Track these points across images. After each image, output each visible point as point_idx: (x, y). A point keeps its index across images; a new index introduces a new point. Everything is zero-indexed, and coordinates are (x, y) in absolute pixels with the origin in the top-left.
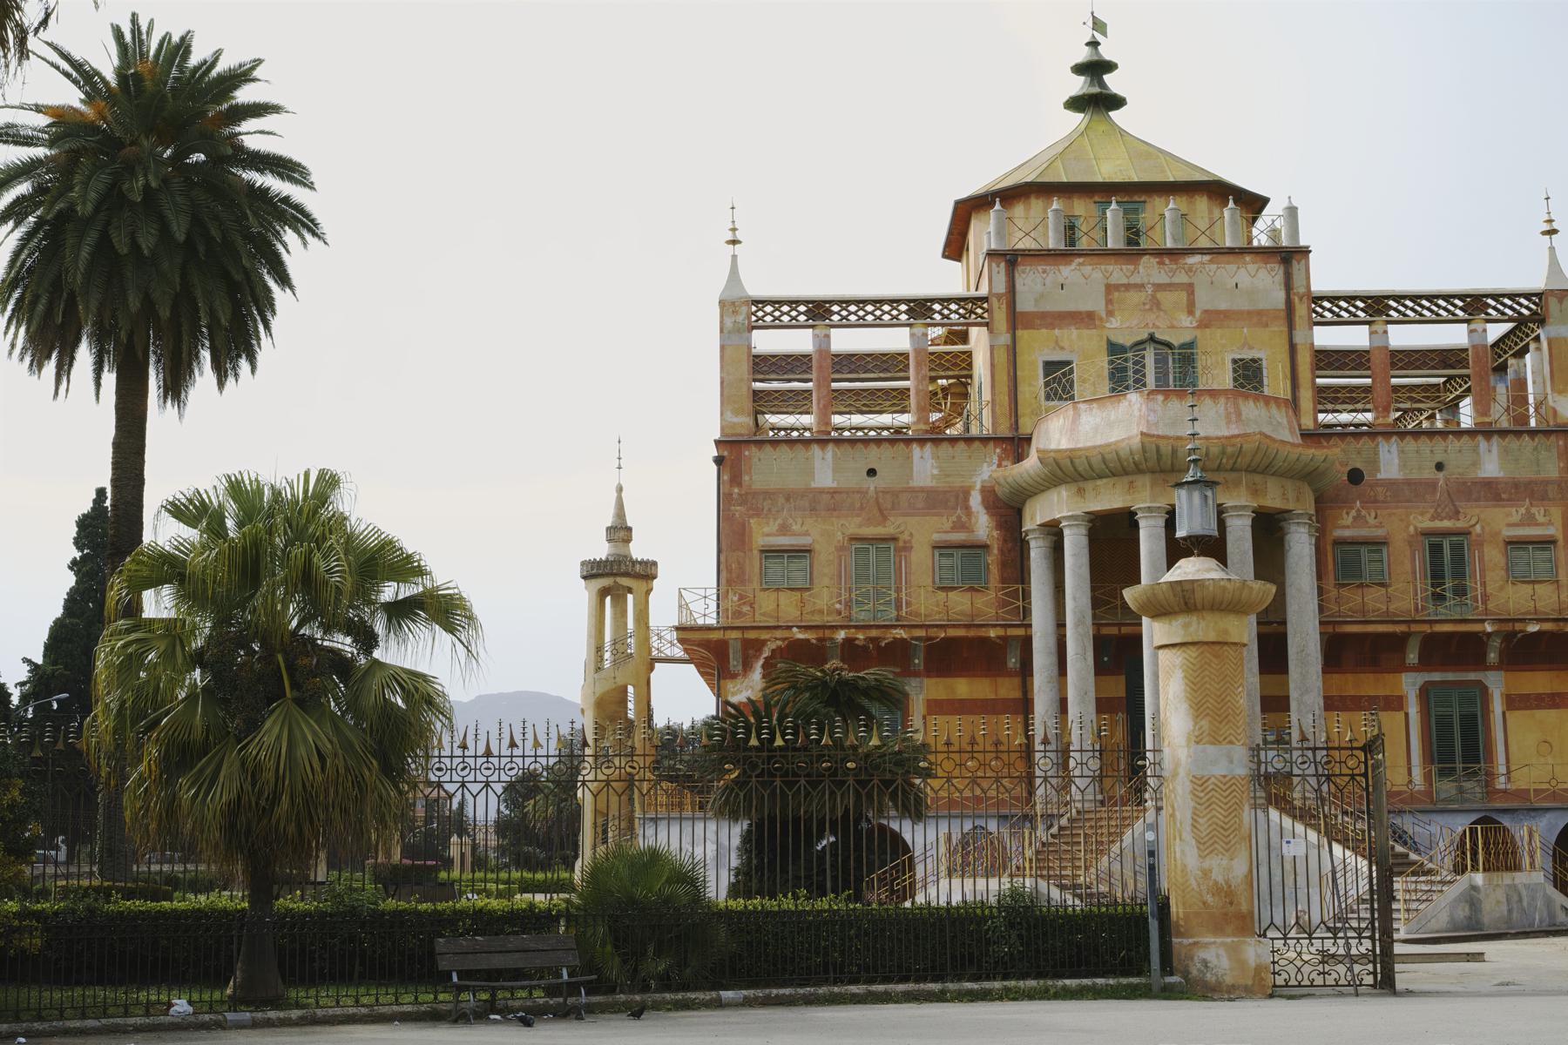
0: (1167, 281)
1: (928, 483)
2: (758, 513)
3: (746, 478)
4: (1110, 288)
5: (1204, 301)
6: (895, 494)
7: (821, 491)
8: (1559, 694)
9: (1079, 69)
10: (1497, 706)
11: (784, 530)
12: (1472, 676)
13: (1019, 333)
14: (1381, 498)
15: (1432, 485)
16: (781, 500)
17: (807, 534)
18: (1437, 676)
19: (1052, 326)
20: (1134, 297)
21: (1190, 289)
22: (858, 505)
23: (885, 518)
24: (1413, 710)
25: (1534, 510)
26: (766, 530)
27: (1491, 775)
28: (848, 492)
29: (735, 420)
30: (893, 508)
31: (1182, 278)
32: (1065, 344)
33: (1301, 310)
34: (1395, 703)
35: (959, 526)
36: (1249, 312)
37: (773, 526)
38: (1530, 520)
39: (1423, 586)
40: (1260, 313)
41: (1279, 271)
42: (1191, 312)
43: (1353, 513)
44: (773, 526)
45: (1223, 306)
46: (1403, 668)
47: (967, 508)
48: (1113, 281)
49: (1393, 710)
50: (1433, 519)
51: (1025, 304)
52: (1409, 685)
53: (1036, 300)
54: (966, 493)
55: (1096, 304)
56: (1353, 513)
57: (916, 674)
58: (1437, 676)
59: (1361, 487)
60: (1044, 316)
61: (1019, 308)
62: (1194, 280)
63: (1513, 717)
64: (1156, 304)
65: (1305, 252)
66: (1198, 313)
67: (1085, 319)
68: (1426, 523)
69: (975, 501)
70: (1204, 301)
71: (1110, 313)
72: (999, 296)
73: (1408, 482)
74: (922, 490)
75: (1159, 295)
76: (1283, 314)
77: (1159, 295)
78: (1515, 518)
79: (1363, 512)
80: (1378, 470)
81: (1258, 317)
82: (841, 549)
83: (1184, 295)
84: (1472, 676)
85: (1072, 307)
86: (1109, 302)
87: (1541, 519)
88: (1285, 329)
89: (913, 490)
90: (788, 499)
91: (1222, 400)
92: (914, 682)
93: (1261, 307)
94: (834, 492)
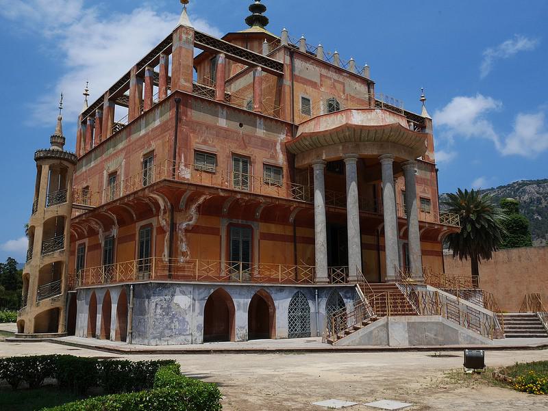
2: (194, 131)
9: (254, 8)
11: (205, 142)
16: (204, 128)
17: (214, 146)
19: (304, 84)
20: (329, 82)
23: (246, 147)
32: (308, 92)
33: (372, 103)
37: (199, 140)
44: (199, 140)
47: (276, 150)
55: (317, 80)
64: (335, 87)
67: (314, 85)
69: (278, 147)
71: (321, 85)
74: (260, 138)
75: (336, 84)
77: (336, 84)
82: (229, 157)
85: (309, 78)
86: (321, 81)
94: (226, 130)
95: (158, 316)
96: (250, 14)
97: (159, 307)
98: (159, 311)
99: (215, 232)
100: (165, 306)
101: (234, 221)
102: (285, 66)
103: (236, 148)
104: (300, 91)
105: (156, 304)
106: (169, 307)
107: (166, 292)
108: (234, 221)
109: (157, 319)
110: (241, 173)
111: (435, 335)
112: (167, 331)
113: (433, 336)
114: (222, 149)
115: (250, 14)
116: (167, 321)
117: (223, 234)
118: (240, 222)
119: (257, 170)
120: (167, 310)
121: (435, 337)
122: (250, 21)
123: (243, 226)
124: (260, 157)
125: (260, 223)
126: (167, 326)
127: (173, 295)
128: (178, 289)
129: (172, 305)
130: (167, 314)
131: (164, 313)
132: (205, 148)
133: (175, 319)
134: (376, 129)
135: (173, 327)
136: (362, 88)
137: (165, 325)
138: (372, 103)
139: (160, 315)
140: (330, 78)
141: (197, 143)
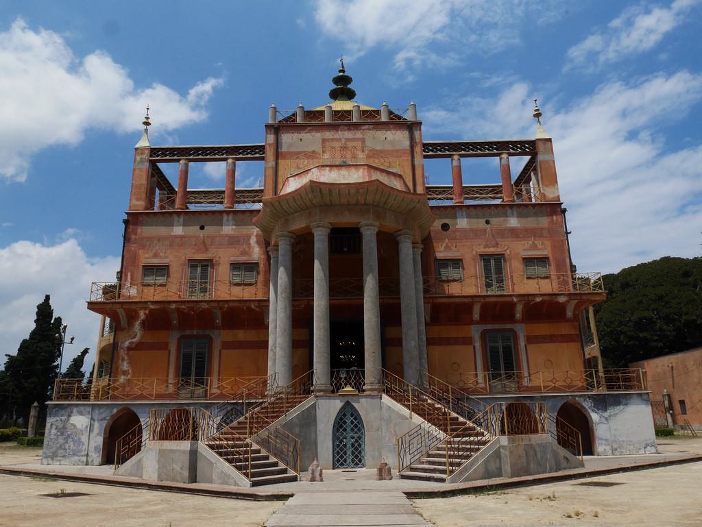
0: (352, 137)
2: (143, 247)
4: (324, 141)
7: (176, 237)
8: (554, 335)
9: (337, 80)
10: (522, 343)
11: (156, 256)
12: (508, 326)
13: (280, 161)
14: (458, 237)
15: (485, 231)
16: (156, 241)
17: (167, 257)
18: (489, 327)
21: (363, 141)
22: (194, 243)
23: (207, 250)
24: (478, 345)
25: (536, 242)
26: (147, 256)
27: (520, 377)
29: (137, 203)
30: (211, 245)
32: (301, 166)
33: (418, 149)
34: (468, 341)
35: (244, 253)
36: (392, 151)
38: (534, 247)
39: (482, 282)
40: (397, 151)
41: (406, 133)
43: (444, 245)
45: (379, 148)
46: (471, 322)
48: (325, 137)
49: (467, 344)
50: (485, 247)
51: (284, 149)
52: (475, 331)
53: (288, 147)
55: (317, 147)
56: (444, 245)
57: (218, 328)
58: (489, 327)
59: (448, 232)
63: (531, 347)
65: (420, 124)
66: (366, 152)
68: (482, 250)
70: (370, 144)
71: (324, 152)
72: (270, 145)
73: (472, 230)
74: (227, 235)
76: (409, 151)
78: (527, 246)
79: (450, 244)
80: (457, 224)
81: (397, 153)
83: (359, 144)
84: (508, 326)
87: (540, 247)
88: (410, 158)
90: (159, 241)
91: (361, 170)
92: (216, 332)
95: (52, 437)
96: (334, 86)
97: (54, 427)
98: (54, 431)
99: (164, 347)
100: (61, 426)
101: (188, 332)
102: (268, 148)
103: (194, 253)
105: (52, 425)
106: (64, 428)
107: (63, 412)
108: (188, 332)
109: (51, 439)
110: (198, 280)
111: (181, 468)
112: (61, 452)
113: (179, 469)
114: (175, 259)
115: (334, 86)
116: (61, 441)
117: (173, 348)
118: (195, 333)
119: (222, 272)
120: (62, 430)
121: (181, 472)
124: (225, 257)
125: (222, 331)
126: (61, 447)
127: (69, 416)
128: (75, 410)
129: (68, 426)
130: (62, 434)
131: (59, 434)
132: (155, 262)
133: (70, 440)
134: (358, 185)
135: (67, 447)
136: (400, 138)
137: (58, 445)
138: (418, 149)
139: (55, 435)
140: (339, 140)
141: (146, 258)
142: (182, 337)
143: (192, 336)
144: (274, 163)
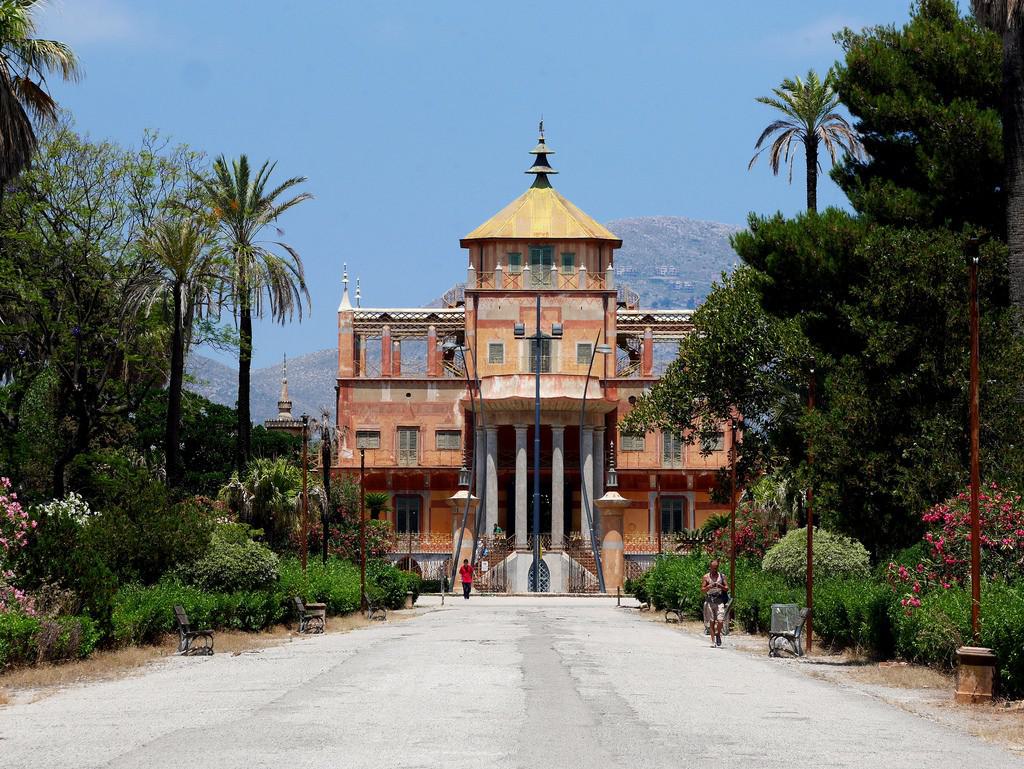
0: (549, 306)
1: (434, 400)
2: (355, 412)
3: (350, 397)
5: (566, 316)
6: (419, 405)
10: (691, 508)
11: (367, 421)
12: (680, 494)
16: (366, 408)
18: (663, 493)
19: (494, 327)
21: (559, 310)
23: (414, 417)
24: (652, 509)
26: (359, 421)
28: (398, 404)
29: (346, 369)
31: (556, 305)
36: (587, 322)
40: (592, 322)
42: (559, 321)
45: (575, 318)
51: (481, 316)
52: (651, 497)
54: (452, 405)
57: (427, 489)
58: (663, 493)
60: (490, 322)
61: (479, 318)
62: (562, 306)
63: (698, 512)
69: (456, 409)
70: (566, 316)
72: (470, 312)
74: (432, 403)
81: (590, 324)
84: (680, 494)
85: (504, 318)
89: (427, 403)
92: (426, 492)
93: (593, 319)
94: (390, 404)
104: (486, 338)
108: (401, 492)
114: (384, 424)
119: (429, 439)
122: (537, 163)
123: (411, 496)
124: (431, 423)
132: (368, 427)
141: (359, 424)
142: (397, 495)
143: (405, 496)
144: (474, 332)
